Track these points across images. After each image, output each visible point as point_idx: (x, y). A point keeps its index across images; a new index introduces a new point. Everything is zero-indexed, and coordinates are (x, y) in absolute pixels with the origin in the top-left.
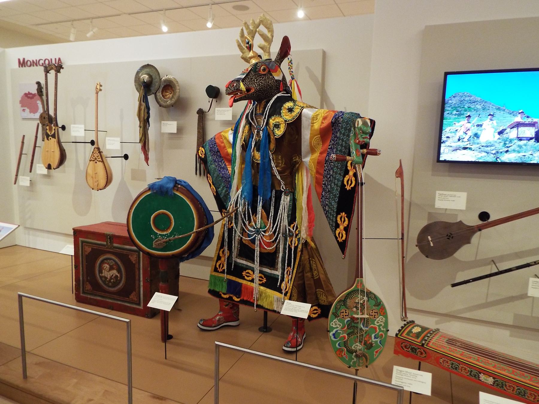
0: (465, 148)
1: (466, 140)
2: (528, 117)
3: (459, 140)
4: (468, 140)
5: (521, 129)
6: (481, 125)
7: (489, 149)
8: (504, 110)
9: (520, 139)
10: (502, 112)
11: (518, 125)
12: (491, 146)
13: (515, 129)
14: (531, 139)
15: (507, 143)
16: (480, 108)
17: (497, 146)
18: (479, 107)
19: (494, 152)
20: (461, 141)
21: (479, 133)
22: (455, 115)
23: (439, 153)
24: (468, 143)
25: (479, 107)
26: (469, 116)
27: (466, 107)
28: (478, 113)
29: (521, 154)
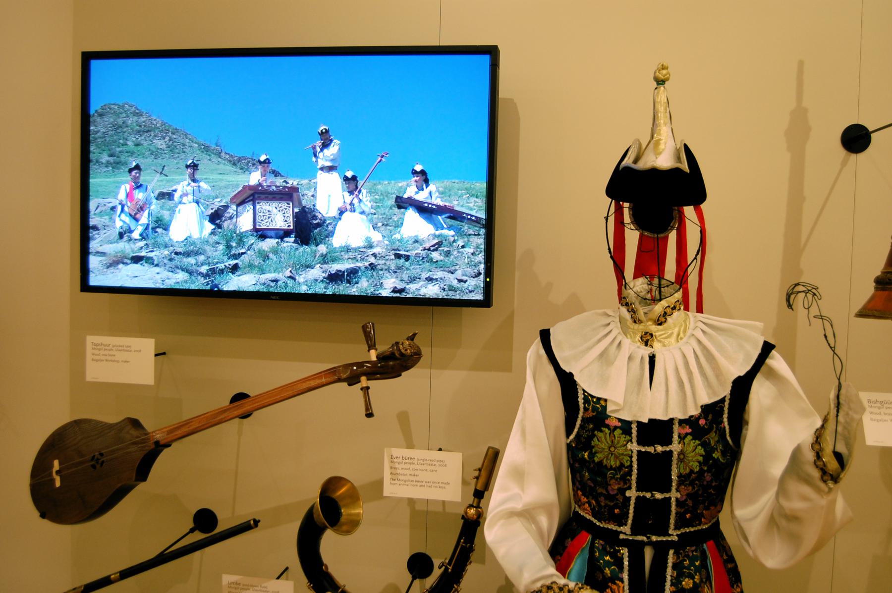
0: (137, 260)
1: (136, 235)
2: (276, 174)
3: (121, 235)
4: (143, 237)
5: (264, 206)
6: (169, 196)
7: (191, 260)
8: (219, 154)
9: (262, 234)
10: (215, 159)
11: (254, 195)
12: (197, 253)
13: (249, 207)
14: (286, 233)
15: (234, 243)
16: (164, 146)
17: (210, 254)
18: (160, 144)
19: (204, 269)
20: (125, 238)
21: (166, 214)
22: (108, 164)
23: (85, 271)
24: (142, 244)
25: (160, 144)
26: (137, 167)
27: (129, 143)
28: (159, 161)
29: (265, 277)
